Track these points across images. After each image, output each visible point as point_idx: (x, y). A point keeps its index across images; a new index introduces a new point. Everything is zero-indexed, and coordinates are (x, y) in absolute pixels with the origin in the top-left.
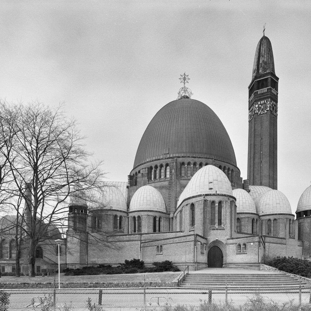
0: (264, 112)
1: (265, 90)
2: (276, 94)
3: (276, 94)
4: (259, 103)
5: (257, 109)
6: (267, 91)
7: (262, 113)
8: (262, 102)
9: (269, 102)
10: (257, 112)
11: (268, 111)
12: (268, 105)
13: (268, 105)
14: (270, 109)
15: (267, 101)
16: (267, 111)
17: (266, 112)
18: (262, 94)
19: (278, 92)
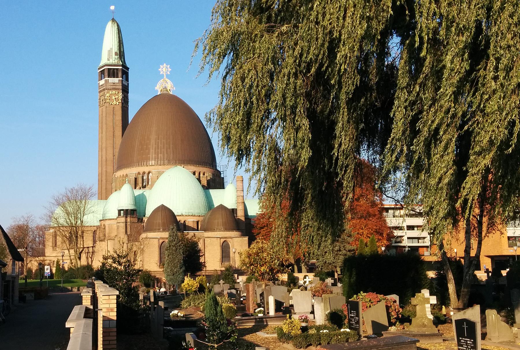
2: (127, 85)
4: (111, 92)
6: (118, 82)
19: (128, 82)
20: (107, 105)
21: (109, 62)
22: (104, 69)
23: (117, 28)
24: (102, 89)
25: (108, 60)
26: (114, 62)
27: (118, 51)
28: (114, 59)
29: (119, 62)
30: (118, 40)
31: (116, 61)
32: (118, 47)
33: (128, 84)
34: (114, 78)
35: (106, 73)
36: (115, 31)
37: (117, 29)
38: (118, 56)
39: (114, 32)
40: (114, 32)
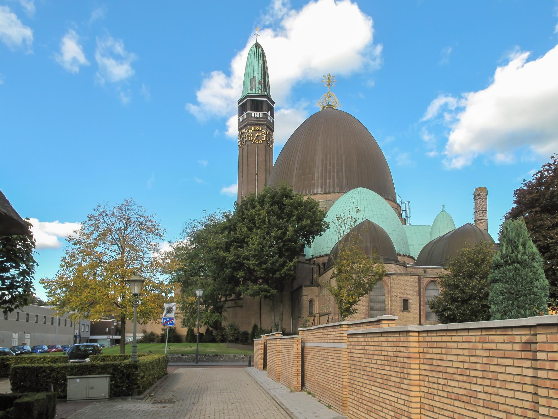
0: (259, 141)
1: (260, 114)
2: (272, 122)
3: (272, 122)
4: (253, 128)
5: (250, 135)
6: (262, 116)
7: (257, 142)
8: (256, 128)
9: (264, 131)
10: (250, 139)
11: (263, 142)
12: (264, 134)
13: (264, 134)
14: (266, 139)
15: (262, 129)
16: (263, 141)
17: (262, 142)
18: (257, 118)
20: (249, 143)
21: (251, 92)
22: (246, 102)
23: (261, 53)
24: (243, 125)
25: (251, 90)
26: (257, 92)
27: (263, 80)
28: (257, 89)
29: (263, 93)
30: (262, 67)
31: (260, 92)
32: (263, 75)
33: (273, 121)
34: (258, 111)
35: (248, 106)
36: (259, 56)
37: (261, 55)
38: (263, 86)
39: (257, 57)
40: (257, 57)
